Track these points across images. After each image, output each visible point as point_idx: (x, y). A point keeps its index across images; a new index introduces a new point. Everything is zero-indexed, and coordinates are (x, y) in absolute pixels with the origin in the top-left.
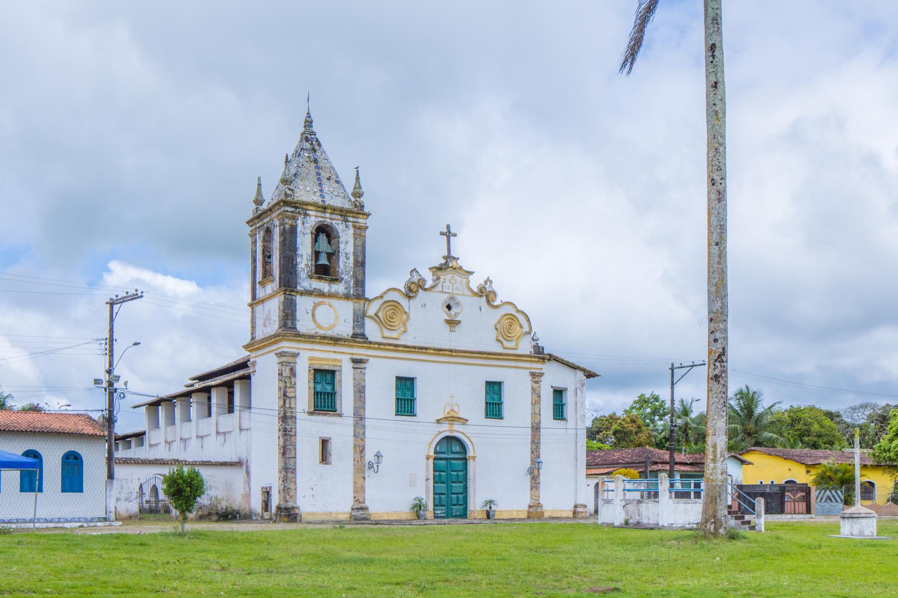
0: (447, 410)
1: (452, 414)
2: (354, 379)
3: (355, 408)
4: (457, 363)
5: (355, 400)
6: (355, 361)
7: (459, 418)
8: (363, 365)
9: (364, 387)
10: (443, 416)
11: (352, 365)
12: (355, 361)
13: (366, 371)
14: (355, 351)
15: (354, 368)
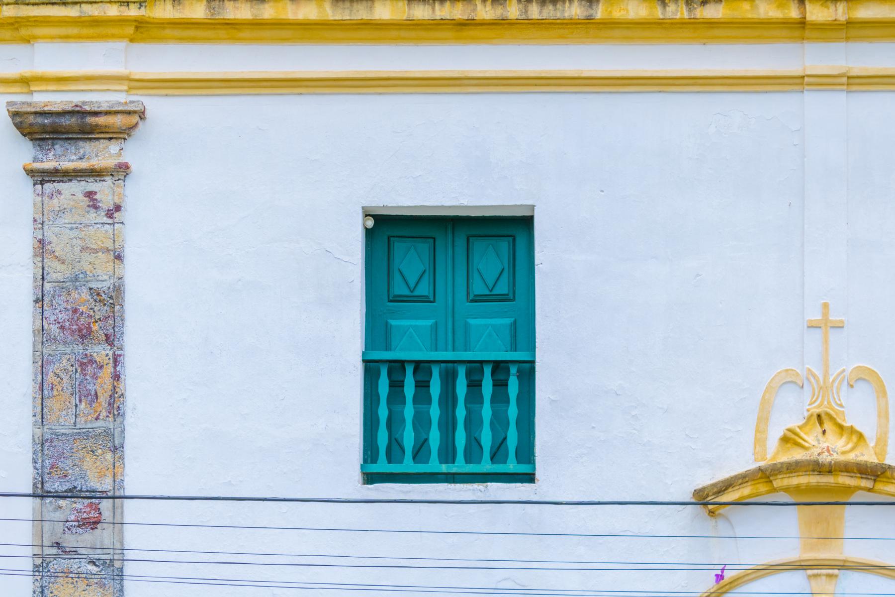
0: (790, 413)
1: (832, 447)
2: (42, 247)
3: (42, 444)
4: (853, 82)
5: (43, 389)
6: (44, 129)
7: (875, 473)
8: (102, 154)
9: (112, 299)
10: (746, 464)
11: (24, 153)
12: (44, 129)
13: (137, 196)
14: (51, 58)
15: (41, 177)
